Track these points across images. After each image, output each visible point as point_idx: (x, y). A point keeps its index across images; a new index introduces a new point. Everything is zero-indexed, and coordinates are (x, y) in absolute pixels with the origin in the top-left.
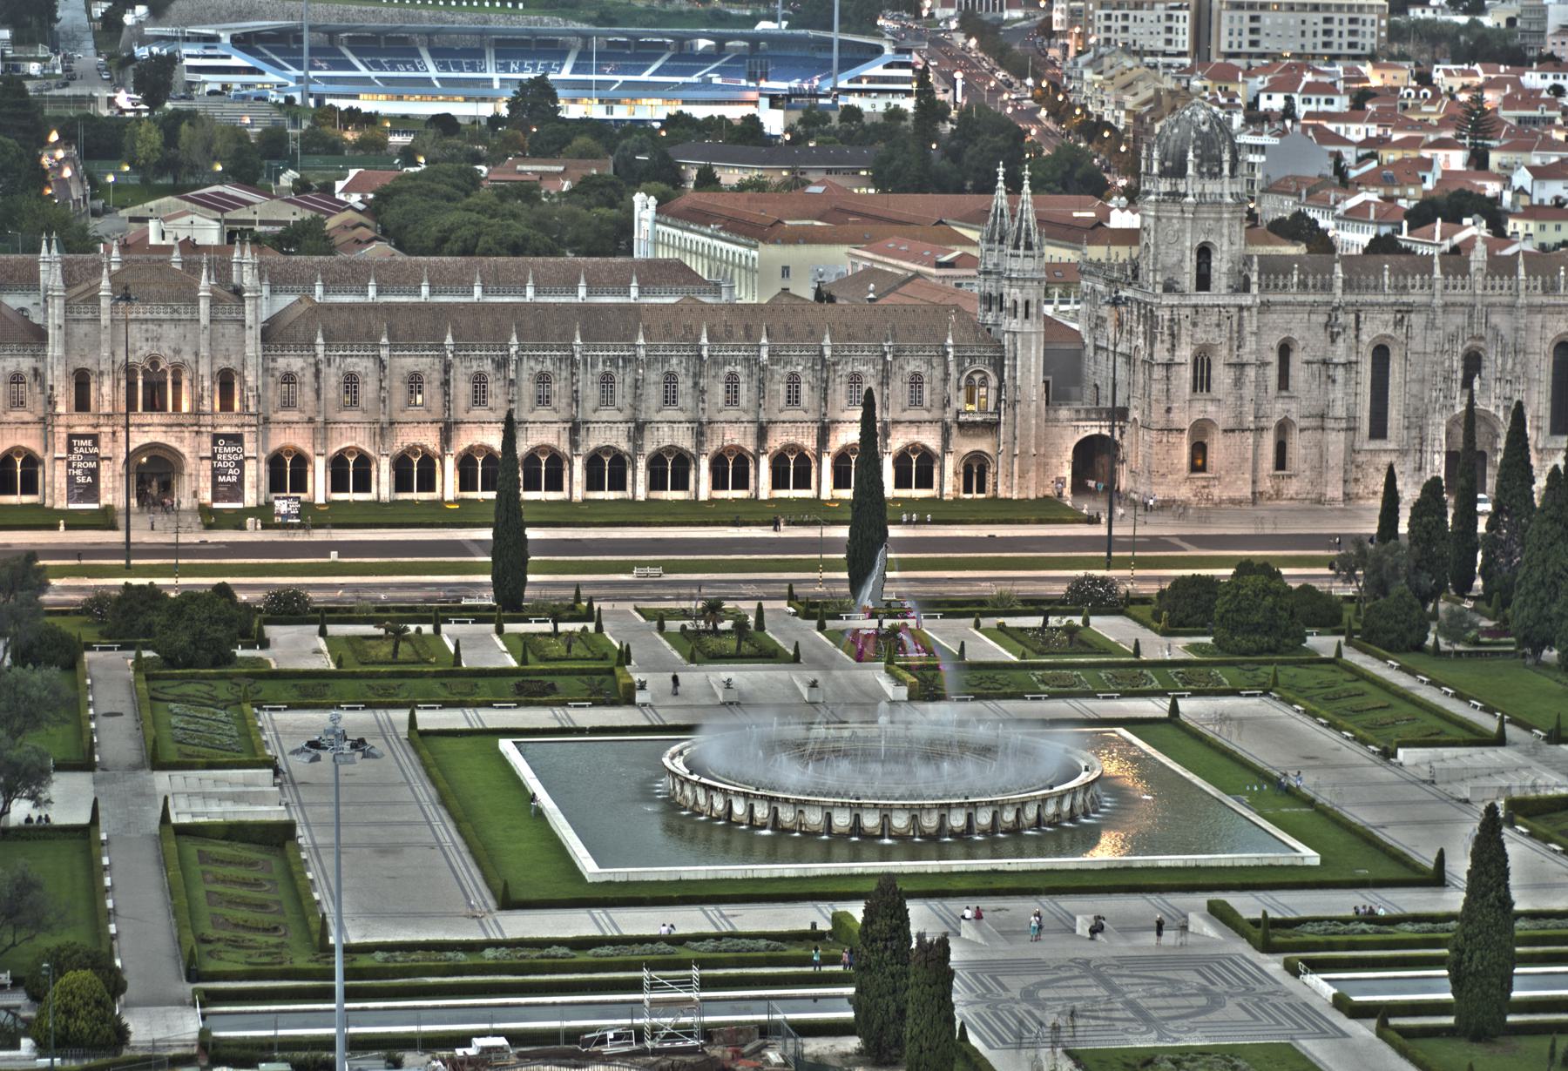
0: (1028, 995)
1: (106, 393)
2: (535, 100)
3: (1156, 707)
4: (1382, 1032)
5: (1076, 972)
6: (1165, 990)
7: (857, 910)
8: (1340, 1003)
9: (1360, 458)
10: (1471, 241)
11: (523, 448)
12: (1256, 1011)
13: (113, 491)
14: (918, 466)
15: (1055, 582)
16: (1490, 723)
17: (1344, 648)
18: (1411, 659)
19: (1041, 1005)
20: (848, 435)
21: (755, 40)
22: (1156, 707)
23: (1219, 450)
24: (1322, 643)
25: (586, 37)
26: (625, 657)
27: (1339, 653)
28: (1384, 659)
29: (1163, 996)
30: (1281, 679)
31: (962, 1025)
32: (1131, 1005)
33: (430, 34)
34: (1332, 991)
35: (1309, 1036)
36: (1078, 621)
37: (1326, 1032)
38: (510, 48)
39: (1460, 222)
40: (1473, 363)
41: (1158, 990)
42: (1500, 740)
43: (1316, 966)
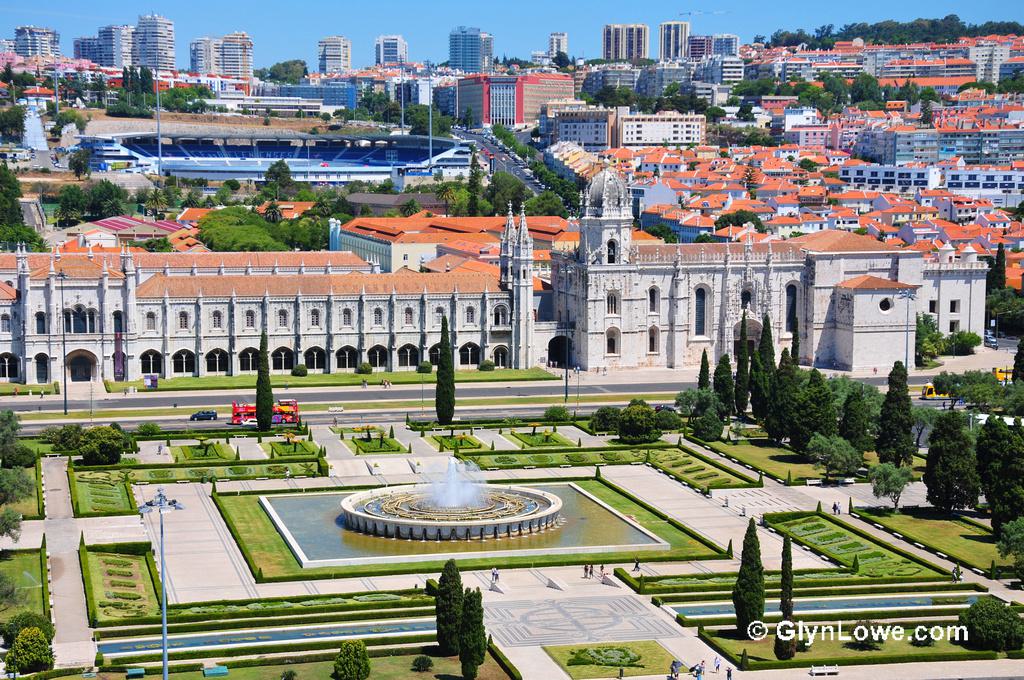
0: (524, 619)
1: (56, 324)
2: (279, 174)
3: (590, 472)
4: (700, 636)
5: (547, 607)
6: (593, 615)
7: (436, 577)
8: (679, 620)
9: (691, 345)
10: (745, 237)
11: (271, 348)
12: (638, 624)
13: (57, 370)
14: (472, 354)
15: (538, 408)
16: (755, 476)
17: (682, 440)
18: (717, 445)
19: (529, 623)
20: (434, 340)
21: (390, 140)
22: (590, 472)
23: (624, 342)
24: (671, 437)
25: (305, 140)
26: (322, 453)
27: (680, 442)
28: (702, 445)
29: (592, 617)
30: (651, 456)
31: (490, 636)
32: (575, 623)
33: (225, 139)
34: (675, 614)
35: (664, 636)
36: (550, 429)
37: (671, 634)
38: (266, 147)
39: (741, 226)
40: (747, 296)
41: (589, 615)
42: (760, 484)
43: (667, 600)
